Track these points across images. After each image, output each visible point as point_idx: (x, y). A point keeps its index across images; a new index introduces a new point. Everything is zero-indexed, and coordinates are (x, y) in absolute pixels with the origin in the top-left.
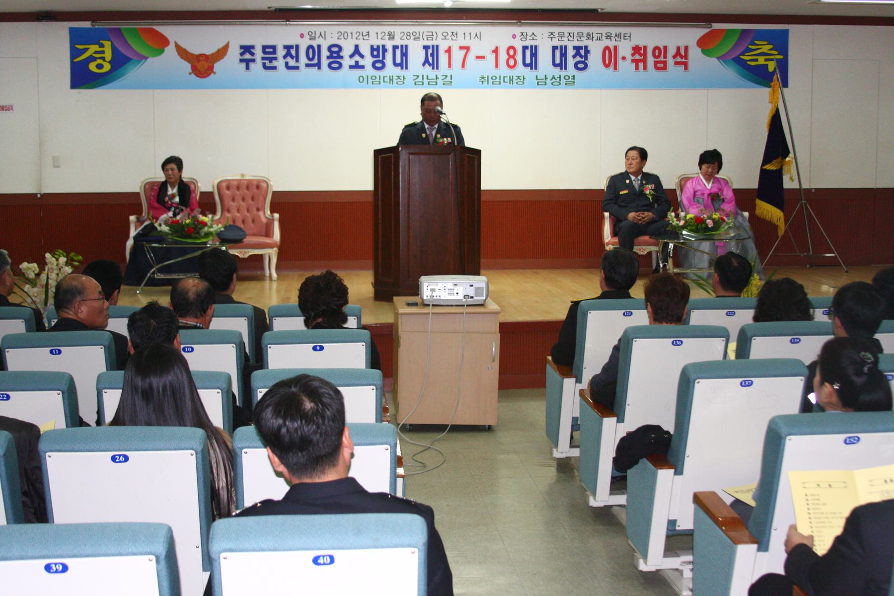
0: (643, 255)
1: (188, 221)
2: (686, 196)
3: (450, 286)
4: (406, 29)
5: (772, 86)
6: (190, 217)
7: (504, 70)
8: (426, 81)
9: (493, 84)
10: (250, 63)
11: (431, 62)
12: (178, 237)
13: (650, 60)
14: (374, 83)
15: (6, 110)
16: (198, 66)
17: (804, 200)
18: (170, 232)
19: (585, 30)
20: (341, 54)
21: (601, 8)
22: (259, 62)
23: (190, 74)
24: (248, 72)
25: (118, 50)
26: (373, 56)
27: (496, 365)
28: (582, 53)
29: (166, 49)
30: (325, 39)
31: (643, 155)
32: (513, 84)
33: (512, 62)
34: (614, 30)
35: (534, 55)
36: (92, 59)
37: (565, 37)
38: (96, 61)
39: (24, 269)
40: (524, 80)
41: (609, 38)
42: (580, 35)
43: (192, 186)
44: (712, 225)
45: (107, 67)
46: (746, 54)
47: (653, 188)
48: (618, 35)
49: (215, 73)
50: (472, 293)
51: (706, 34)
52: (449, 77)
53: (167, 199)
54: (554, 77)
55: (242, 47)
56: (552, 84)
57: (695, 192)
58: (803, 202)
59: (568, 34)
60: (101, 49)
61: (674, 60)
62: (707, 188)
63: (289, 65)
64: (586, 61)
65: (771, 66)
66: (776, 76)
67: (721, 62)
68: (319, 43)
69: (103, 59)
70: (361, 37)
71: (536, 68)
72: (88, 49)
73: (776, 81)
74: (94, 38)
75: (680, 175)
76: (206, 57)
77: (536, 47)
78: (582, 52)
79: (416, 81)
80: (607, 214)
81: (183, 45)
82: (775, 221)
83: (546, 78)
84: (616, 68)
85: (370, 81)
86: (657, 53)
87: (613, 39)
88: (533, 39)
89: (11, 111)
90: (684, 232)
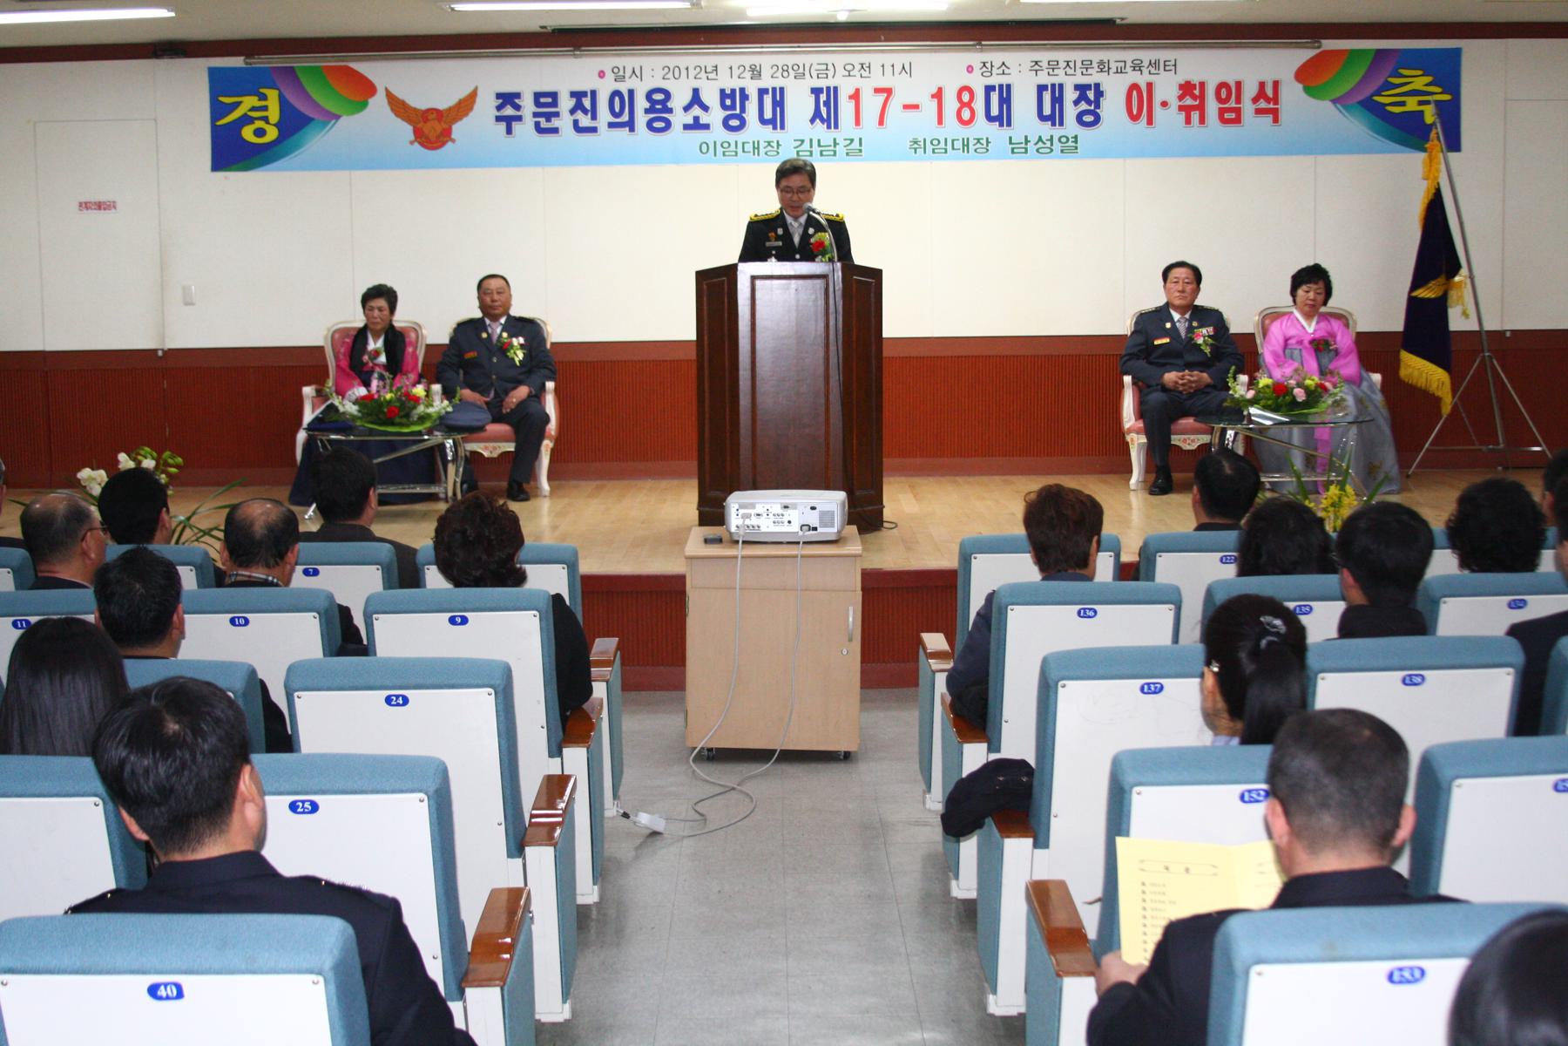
0: (1192, 451)
1: (389, 396)
2: (1271, 348)
3: (777, 509)
4: (781, 60)
5: (1429, 150)
6: (394, 389)
7: (952, 129)
9: (934, 152)
10: (513, 123)
11: (825, 116)
12: (372, 423)
13: (1212, 106)
14: (727, 154)
15: (105, 209)
16: (424, 129)
17: (1489, 351)
18: (360, 415)
19: (1096, 56)
20: (669, 105)
21: (1121, 16)
23: (412, 143)
24: (509, 139)
25: (288, 102)
27: (856, 646)
28: (1090, 96)
29: (371, 101)
31: (1197, 275)
32: (968, 152)
33: (966, 114)
34: (1146, 56)
35: (1006, 100)
36: (246, 120)
38: (253, 123)
39: (86, 480)
40: (987, 145)
41: (1137, 68)
42: (1087, 65)
43: (413, 335)
44: (1304, 398)
45: (272, 134)
46: (1383, 93)
47: (1212, 333)
48: (1154, 64)
49: (453, 141)
50: (814, 522)
51: (1309, 61)
52: (856, 142)
53: (366, 358)
54: (1040, 139)
55: (499, 96)
56: (1037, 151)
57: (1286, 340)
58: (1487, 354)
59: (1066, 64)
60: (263, 103)
61: (1255, 106)
62: (1306, 332)
63: (581, 125)
64: (1098, 111)
65: (1430, 115)
66: (1434, 131)
67: (1338, 109)
68: (631, 88)
69: (266, 119)
70: (703, 75)
71: (1009, 124)
72: (239, 104)
73: (1436, 142)
74: (250, 84)
75: (1262, 309)
76: (438, 114)
77: (1009, 86)
78: (1091, 95)
79: (798, 149)
80: (1127, 379)
81: (400, 93)
82: (1433, 388)
83: (1027, 141)
84: (1150, 122)
85: (720, 150)
86: (1224, 93)
87: (1145, 71)
88: (1003, 74)
89: (113, 210)
90: (1253, 410)
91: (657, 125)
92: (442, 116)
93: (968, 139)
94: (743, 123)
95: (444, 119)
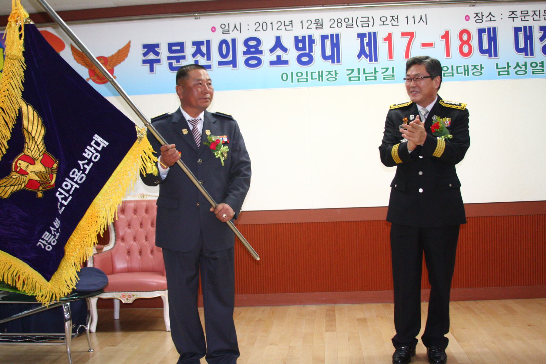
8: (362, 76)
10: (155, 64)
11: (368, 53)
20: (260, 48)
22: (165, 62)
24: (152, 75)
26: (297, 48)
30: (241, 32)
32: (468, 75)
33: (466, 49)
35: (493, 39)
37: (529, 16)
40: (481, 70)
54: (518, 65)
55: (145, 46)
56: (516, 73)
59: (533, 12)
70: (282, 27)
71: (496, 55)
77: (494, 29)
83: (509, 67)
88: (490, 20)
91: (251, 62)
92: (108, 62)
93: (468, 66)
94: (311, 60)
95: (109, 63)
